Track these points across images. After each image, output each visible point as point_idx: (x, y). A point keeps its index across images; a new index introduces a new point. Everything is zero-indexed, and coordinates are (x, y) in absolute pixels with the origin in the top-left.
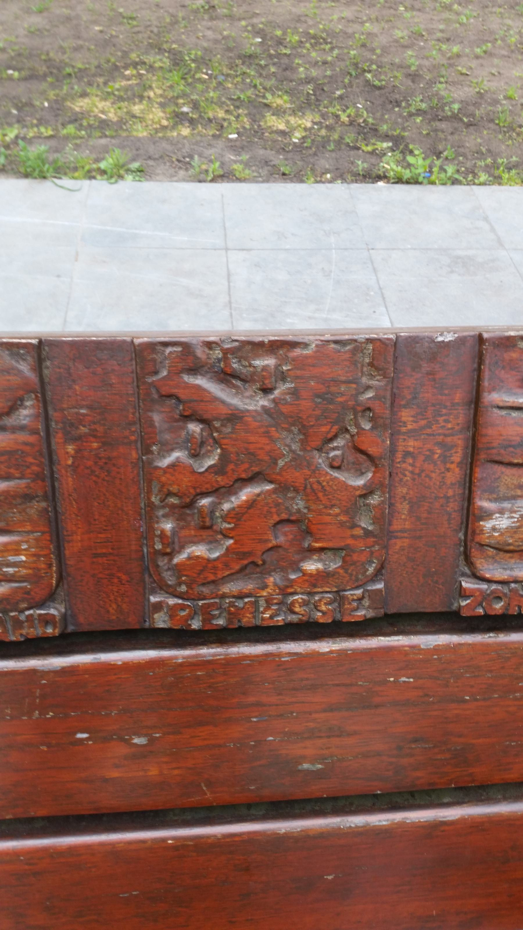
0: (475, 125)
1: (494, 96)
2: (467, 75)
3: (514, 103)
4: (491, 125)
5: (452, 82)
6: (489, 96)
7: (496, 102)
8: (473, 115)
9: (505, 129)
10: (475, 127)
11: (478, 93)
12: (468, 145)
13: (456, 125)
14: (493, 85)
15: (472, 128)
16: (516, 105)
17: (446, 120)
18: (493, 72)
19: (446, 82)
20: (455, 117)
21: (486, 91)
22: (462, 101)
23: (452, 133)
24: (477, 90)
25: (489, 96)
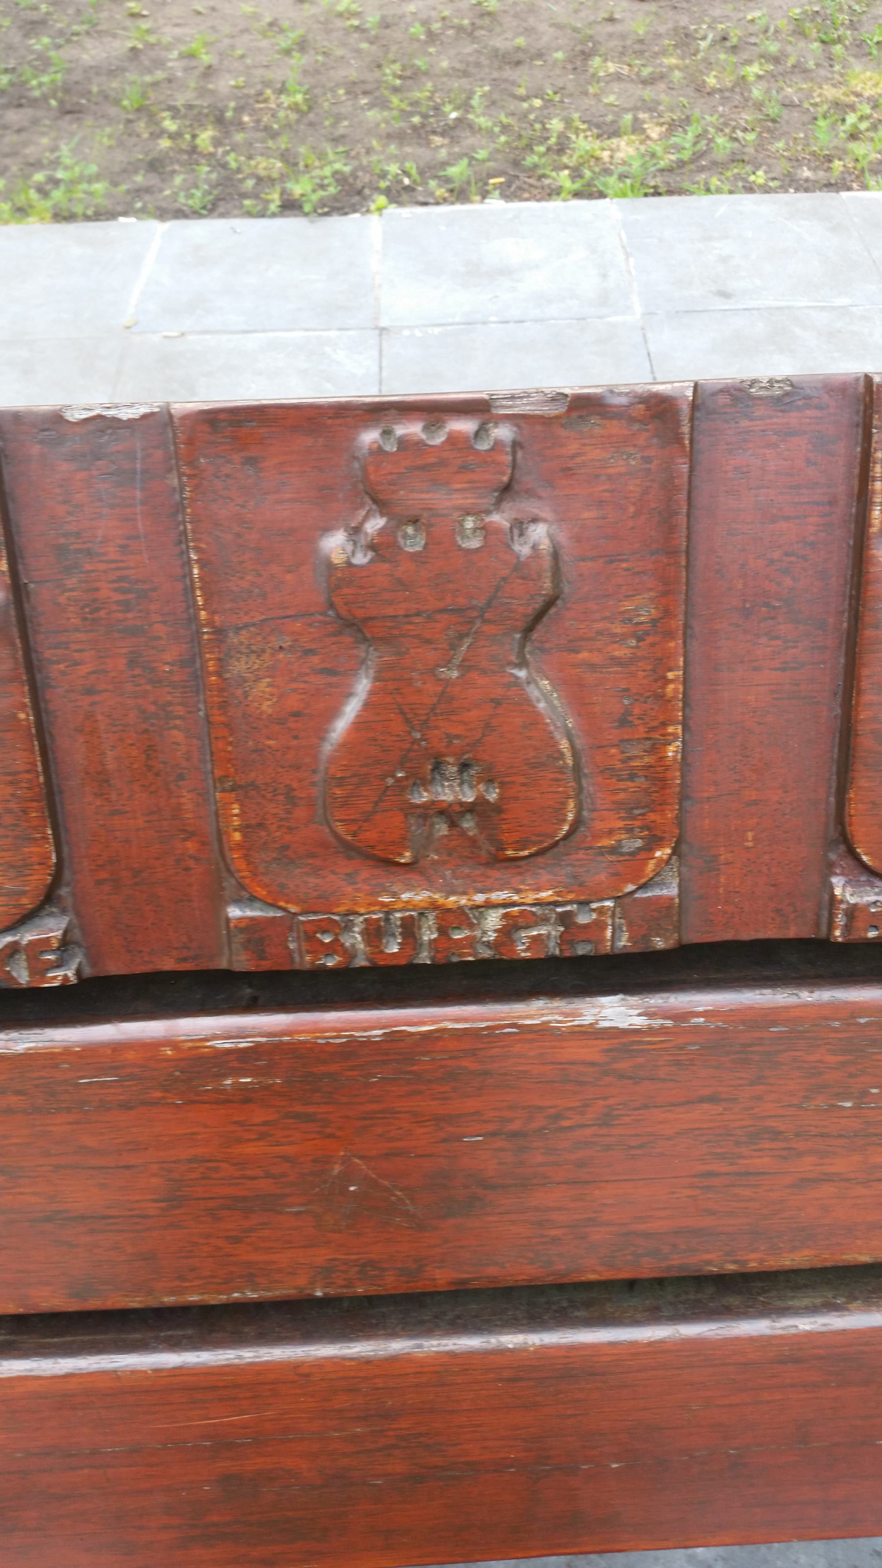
0: (80, 112)
1: (164, 54)
2: (144, 16)
3: (194, 63)
4: (113, 111)
5: (98, 32)
6: (152, 54)
7: (159, 63)
8: (90, 92)
9: (131, 117)
10: (76, 115)
11: (133, 49)
12: (27, 151)
13: (40, 113)
14: (168, 34)
15: (68, 117)
16: (195, 67)
17: (30, 106)
18: (200, 8)
19: (88, 33)
20: (45, 98)
21: (152, 46)
22: (91, 67)
23: (19, 131)
24: (130, 44)
25: (152, 54)
